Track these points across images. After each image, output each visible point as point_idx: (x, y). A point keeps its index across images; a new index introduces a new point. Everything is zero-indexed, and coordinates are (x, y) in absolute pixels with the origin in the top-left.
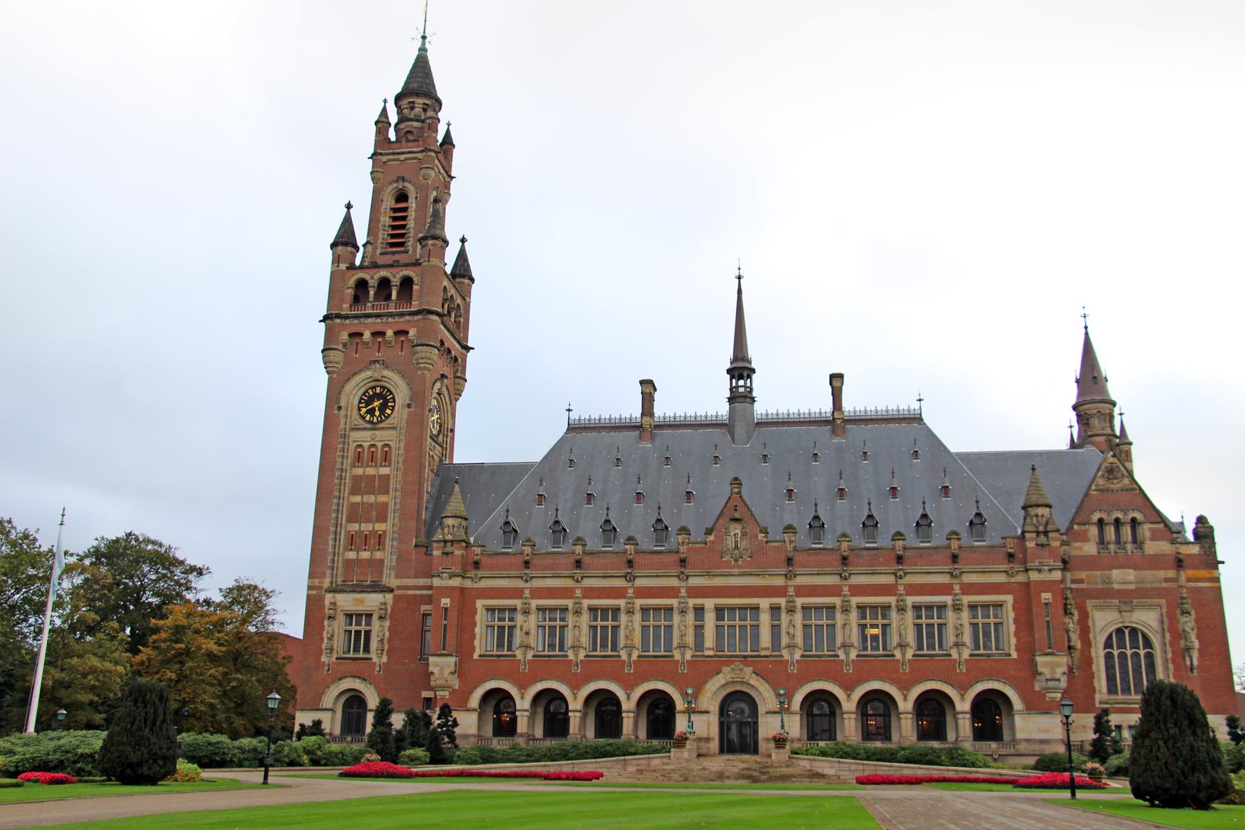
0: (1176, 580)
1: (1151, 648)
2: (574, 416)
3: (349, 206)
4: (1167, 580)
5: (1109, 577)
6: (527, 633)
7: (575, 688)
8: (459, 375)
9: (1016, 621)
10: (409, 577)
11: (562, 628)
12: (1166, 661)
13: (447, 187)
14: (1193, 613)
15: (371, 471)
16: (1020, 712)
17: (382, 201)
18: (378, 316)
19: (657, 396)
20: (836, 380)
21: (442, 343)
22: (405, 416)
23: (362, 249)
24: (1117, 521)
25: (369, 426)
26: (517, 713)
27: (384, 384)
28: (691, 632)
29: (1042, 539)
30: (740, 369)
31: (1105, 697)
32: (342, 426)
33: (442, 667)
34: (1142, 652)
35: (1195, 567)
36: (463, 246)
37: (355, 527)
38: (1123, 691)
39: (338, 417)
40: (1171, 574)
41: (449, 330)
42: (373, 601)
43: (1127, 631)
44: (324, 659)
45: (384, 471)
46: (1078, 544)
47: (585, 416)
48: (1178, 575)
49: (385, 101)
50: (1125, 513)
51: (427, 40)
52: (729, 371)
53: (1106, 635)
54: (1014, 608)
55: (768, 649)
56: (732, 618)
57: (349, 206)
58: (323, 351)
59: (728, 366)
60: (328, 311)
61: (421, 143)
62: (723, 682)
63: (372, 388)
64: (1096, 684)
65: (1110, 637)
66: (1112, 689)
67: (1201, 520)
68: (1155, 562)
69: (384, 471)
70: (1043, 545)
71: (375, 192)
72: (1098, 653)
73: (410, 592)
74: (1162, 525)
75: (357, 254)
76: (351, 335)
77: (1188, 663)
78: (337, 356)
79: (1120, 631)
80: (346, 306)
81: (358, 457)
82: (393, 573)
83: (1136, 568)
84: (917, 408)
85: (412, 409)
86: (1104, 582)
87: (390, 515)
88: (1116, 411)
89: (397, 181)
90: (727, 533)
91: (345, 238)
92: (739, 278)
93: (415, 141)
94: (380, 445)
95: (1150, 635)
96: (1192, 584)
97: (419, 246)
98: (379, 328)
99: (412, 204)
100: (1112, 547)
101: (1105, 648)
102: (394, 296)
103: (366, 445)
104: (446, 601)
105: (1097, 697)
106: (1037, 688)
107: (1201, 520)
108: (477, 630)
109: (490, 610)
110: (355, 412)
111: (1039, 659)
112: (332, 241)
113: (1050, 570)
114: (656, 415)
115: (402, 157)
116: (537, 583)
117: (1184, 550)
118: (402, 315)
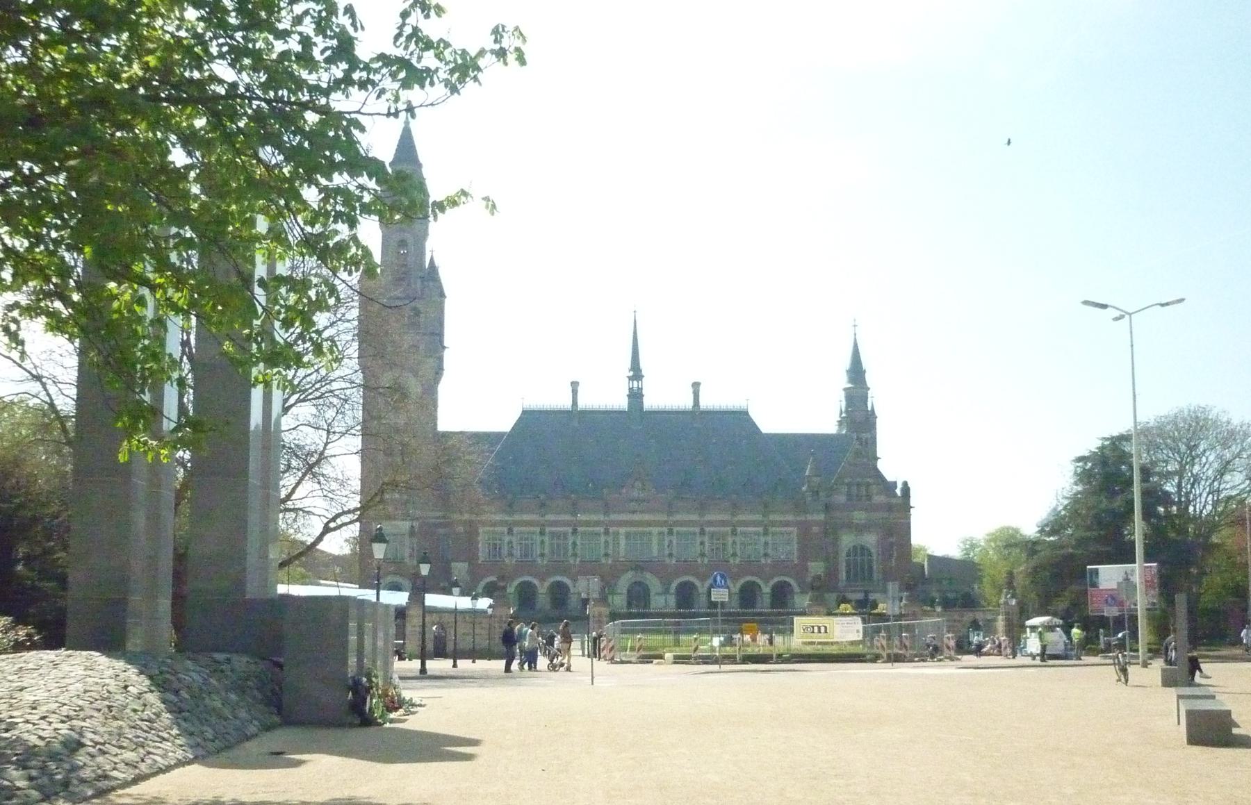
7: (543, 580)
11: (532, 544)
19: (579, 389)
20: (696, 386)
24: (858, 485)
28: (611, 547)
40: (886, 515)
43: (859, 547)
55: (656, 557)
67: (905, 484)
72: (843, 557)
79: (855, 547)
84: (745, 405)
88: (869, 395)
90: (633, 487)
97: (419, 281)
107: (905, 484)
116: (517, 517)
117: (894, 501)
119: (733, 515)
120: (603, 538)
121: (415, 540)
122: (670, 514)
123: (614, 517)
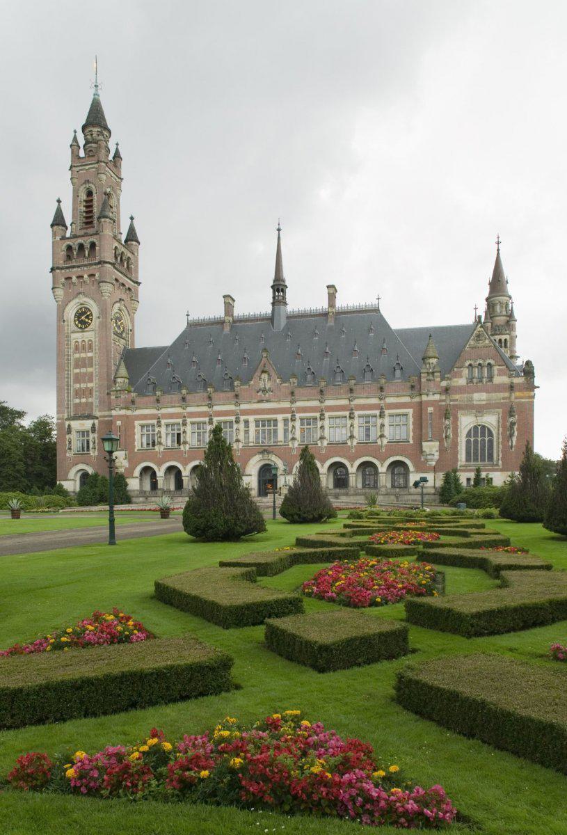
0: (509, 398)
1: (492, 436)
2: (190, 318)
3: (59, 201)
4: (503, 399)
5: (472, 398)
6: (160, 437)
7: (185, 465)
8: (133, 298)
9: (414, 423)
10: (105, 411)
12: (498, 443)
13: (119, 185)
14: (516, 416)
15: (83, 355)
16: (412, 472)
17: (78, 196)
18: (79, 267)
21: (117, 280)
22: (97, 323)
23: (69, 228)
24: (480, 364)
25: (80, 330)
26: (158, 479)
27: (87, 306)
29: (431, 377)
30: (279, 287)
31: (464, 463)
32: (66, 331)
33: (120, 457)
34: (487, 439)
35: (520, 391)
36: (132, 222)
37: (78, 386)
38: (474, 461)
39: (63, 326)
40: (507, 395)
41: (122, 273)
42: (88, 424)
43: (479, 428)
44: (67, 455)
45: (90, 355)
46: (455, 379)
47: (196, 318)
48: (511, 396)
49: (75, 132)
50: (485, 361)
51: (100, 87)
52: (272, 287)
53: (467, 430)
54: (413, 417)
56: (269, 426)
57: (59, 201)
58: (52, 289)
59: (272, 284)
60: (53, 264)
61: (96, 158)
62: (258, 459)
63: (81, 309)
64: (459, 456)
65: (471, 430)
66: (468, 459)
67: (528, 363)
68: (499, 388)
69: (90, 355)
70: (430, 380)
71: (74, 191)
72: (462, 441)
73: (106, 419)
74: (504, 367)
75: (67, 231)
76: (66, 279)
77: (510, 444)
78: (60, 292)
79: (475, 427)
80: (61, 262)
81: (77, 348)
82: (97, 409)
83: (488, 392)
85: (101, 319)
86: (468, 401)
87: (94, 378)
89: (85, 183)
90: (260, 379)
91: (58, 221)
92: (279, 230)
93: (93, 156)
94: (86, 340)
95: (491, 429)
96: (518, 400)
98: (80, 274)
99: (95, 197)
100: (475, 380)
101: (467, 437)
102: (87, 255)
103: (80, 341)
104: (119, 423)
105: (459, 464)
106: (422, 460)
108: (136, 437)
109: (142, 426)
110: (73, 323)
111: (424, 444)
112: (51, 222)
113: (433, 394)
114: (235, 314)
115: (87, 167)
116: (164, 411)
118: (91, 265)
119: (351, 401)
120: (235, 426)
121: (96, 435)
122: (292, 402)
123: (243, 407)
